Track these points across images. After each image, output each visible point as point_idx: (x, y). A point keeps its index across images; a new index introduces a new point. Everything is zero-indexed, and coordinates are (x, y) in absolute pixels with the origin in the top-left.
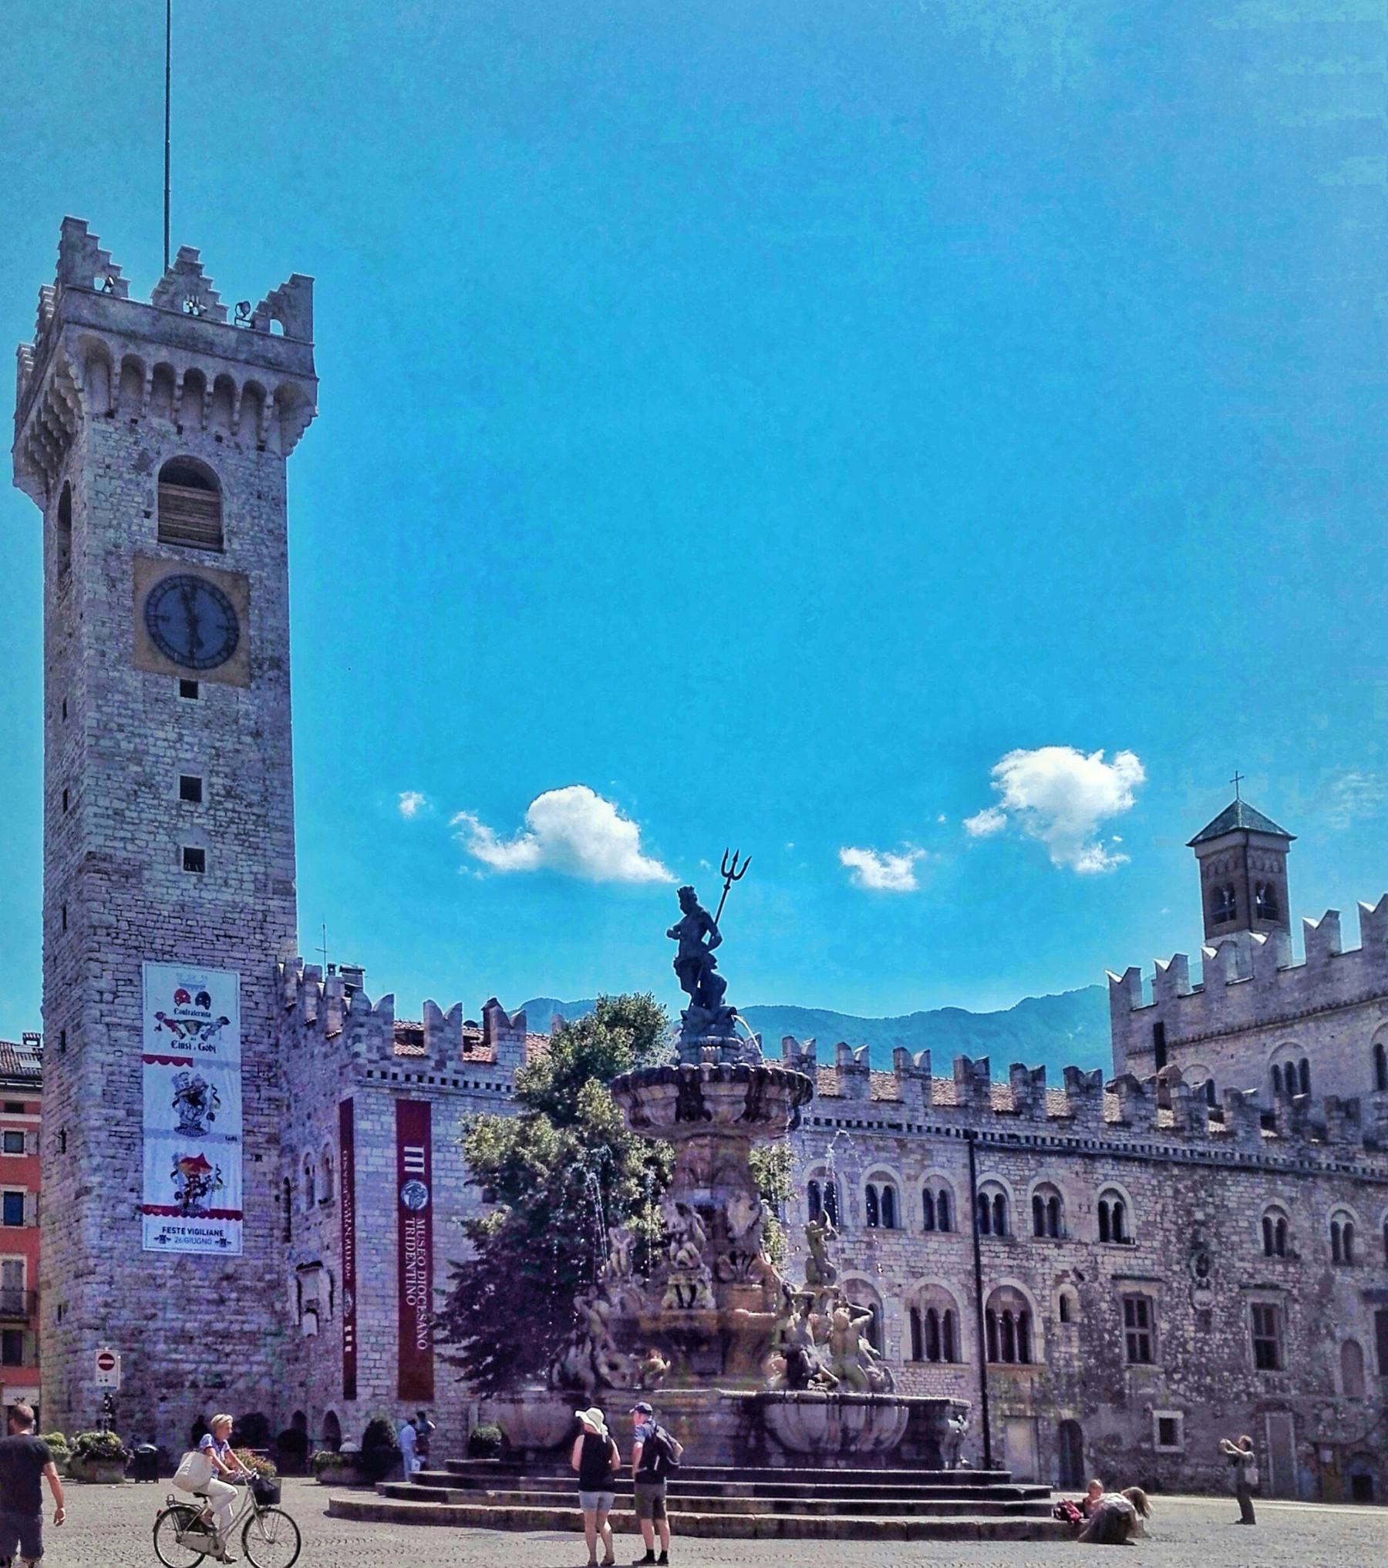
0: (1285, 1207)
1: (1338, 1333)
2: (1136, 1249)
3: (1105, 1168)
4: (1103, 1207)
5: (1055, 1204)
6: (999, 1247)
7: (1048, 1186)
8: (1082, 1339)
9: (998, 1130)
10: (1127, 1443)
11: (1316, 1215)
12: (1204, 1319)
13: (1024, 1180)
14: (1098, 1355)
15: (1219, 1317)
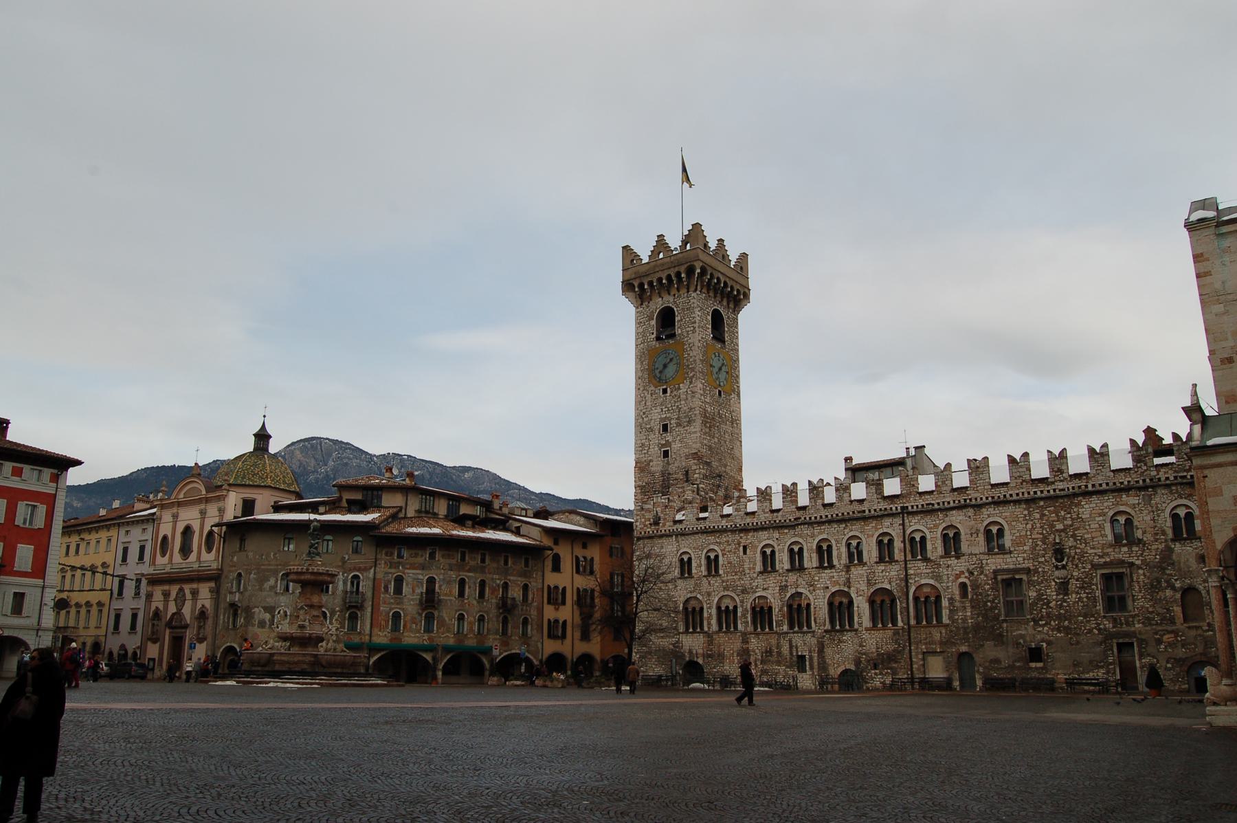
0: (1128, 510)
1: (1178, 585)
2: (1010, 552)
5: (957, 535)
6: (920, 564)
7: (952, 526)
8: (972, 607)
10: (1005, 663)
12: (1063, 587)
13: (936, 526)
14: (985, 617)
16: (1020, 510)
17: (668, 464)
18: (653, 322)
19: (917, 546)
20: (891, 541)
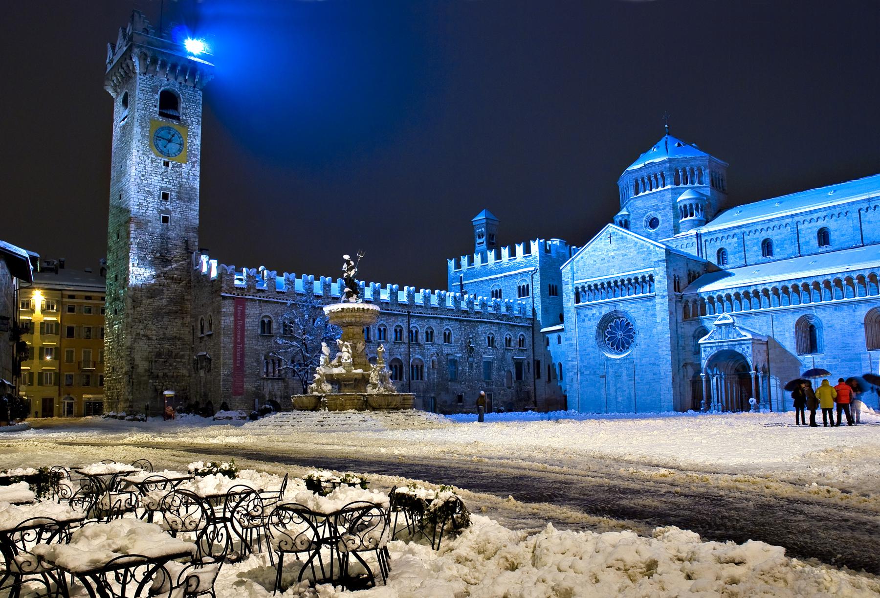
3: (446, 322)
4: (445, 334)
5: (432, 333)
9: (417, 311)
10: (449, 403)
11: (502, 335)
12: (471, 367)
13: (423, 326)
15: (475, 365)
16: (457, 325)
17: (167, 228)
18: (157, 97)
19: (413, 337)
20: (401, 331)
